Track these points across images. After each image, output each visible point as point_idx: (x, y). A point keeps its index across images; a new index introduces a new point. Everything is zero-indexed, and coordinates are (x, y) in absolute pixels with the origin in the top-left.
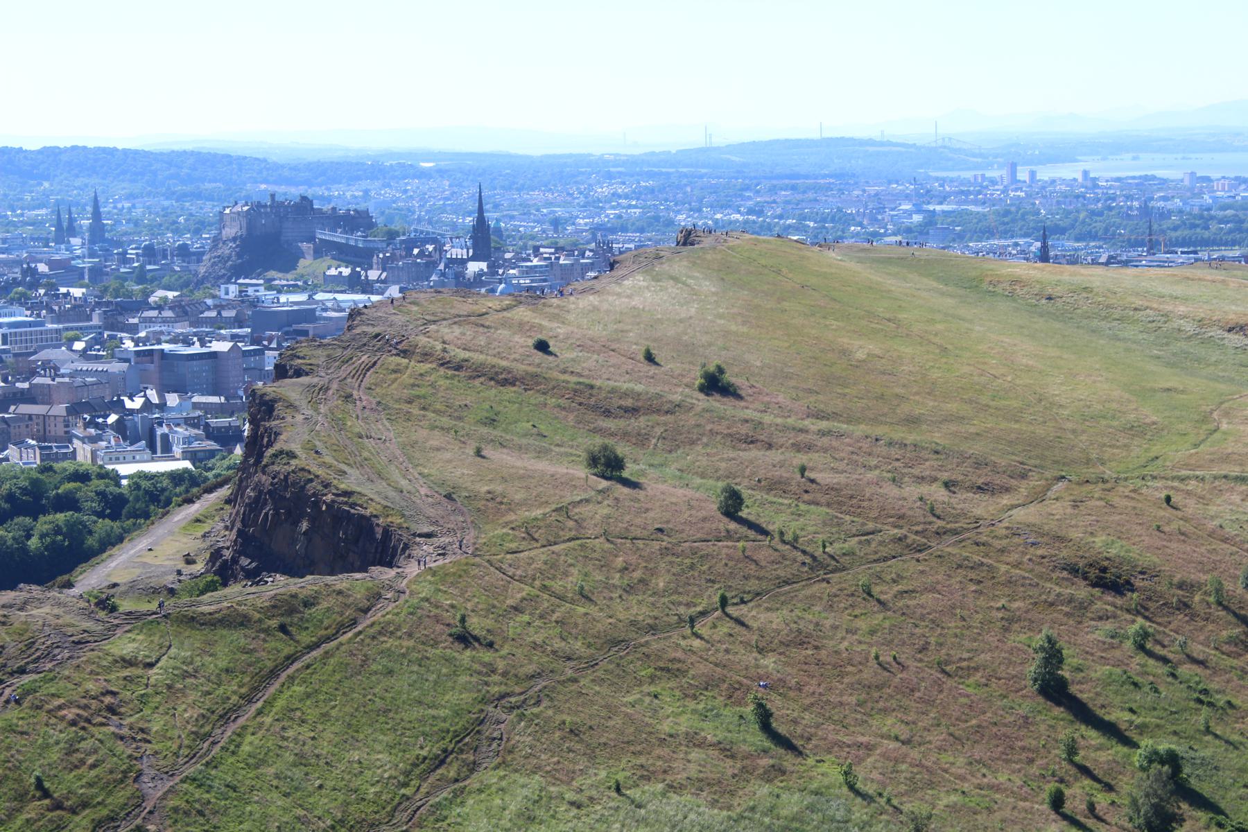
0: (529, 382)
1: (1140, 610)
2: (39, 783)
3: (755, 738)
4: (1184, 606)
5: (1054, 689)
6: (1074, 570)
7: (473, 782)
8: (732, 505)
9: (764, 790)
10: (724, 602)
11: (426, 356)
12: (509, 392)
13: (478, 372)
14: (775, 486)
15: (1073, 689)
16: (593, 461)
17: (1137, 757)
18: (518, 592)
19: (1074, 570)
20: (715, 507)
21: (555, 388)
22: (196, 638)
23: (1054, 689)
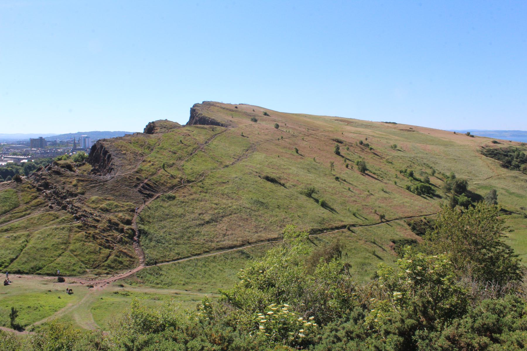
0: (236, 111)
1: (345, 146)
2: (181, 141)
3: (296, 154)
4: (351, 146)
5: (338, 153)
6: (333, 140)
7: (255, 153)
8: (277, 126)
9: (301, 160)
10: (282, 138)
11: (218, 107)
12: (233, 112)
13: (227, 109)
14: (281, 126)
15: (341, 154)
16: (252, 120)
17: (355, 163)
18: (249, 133)
19: (333, 140)
20: (274, 127)
21: (241, 112)
22: (199, 130)
23: (338, 153)
